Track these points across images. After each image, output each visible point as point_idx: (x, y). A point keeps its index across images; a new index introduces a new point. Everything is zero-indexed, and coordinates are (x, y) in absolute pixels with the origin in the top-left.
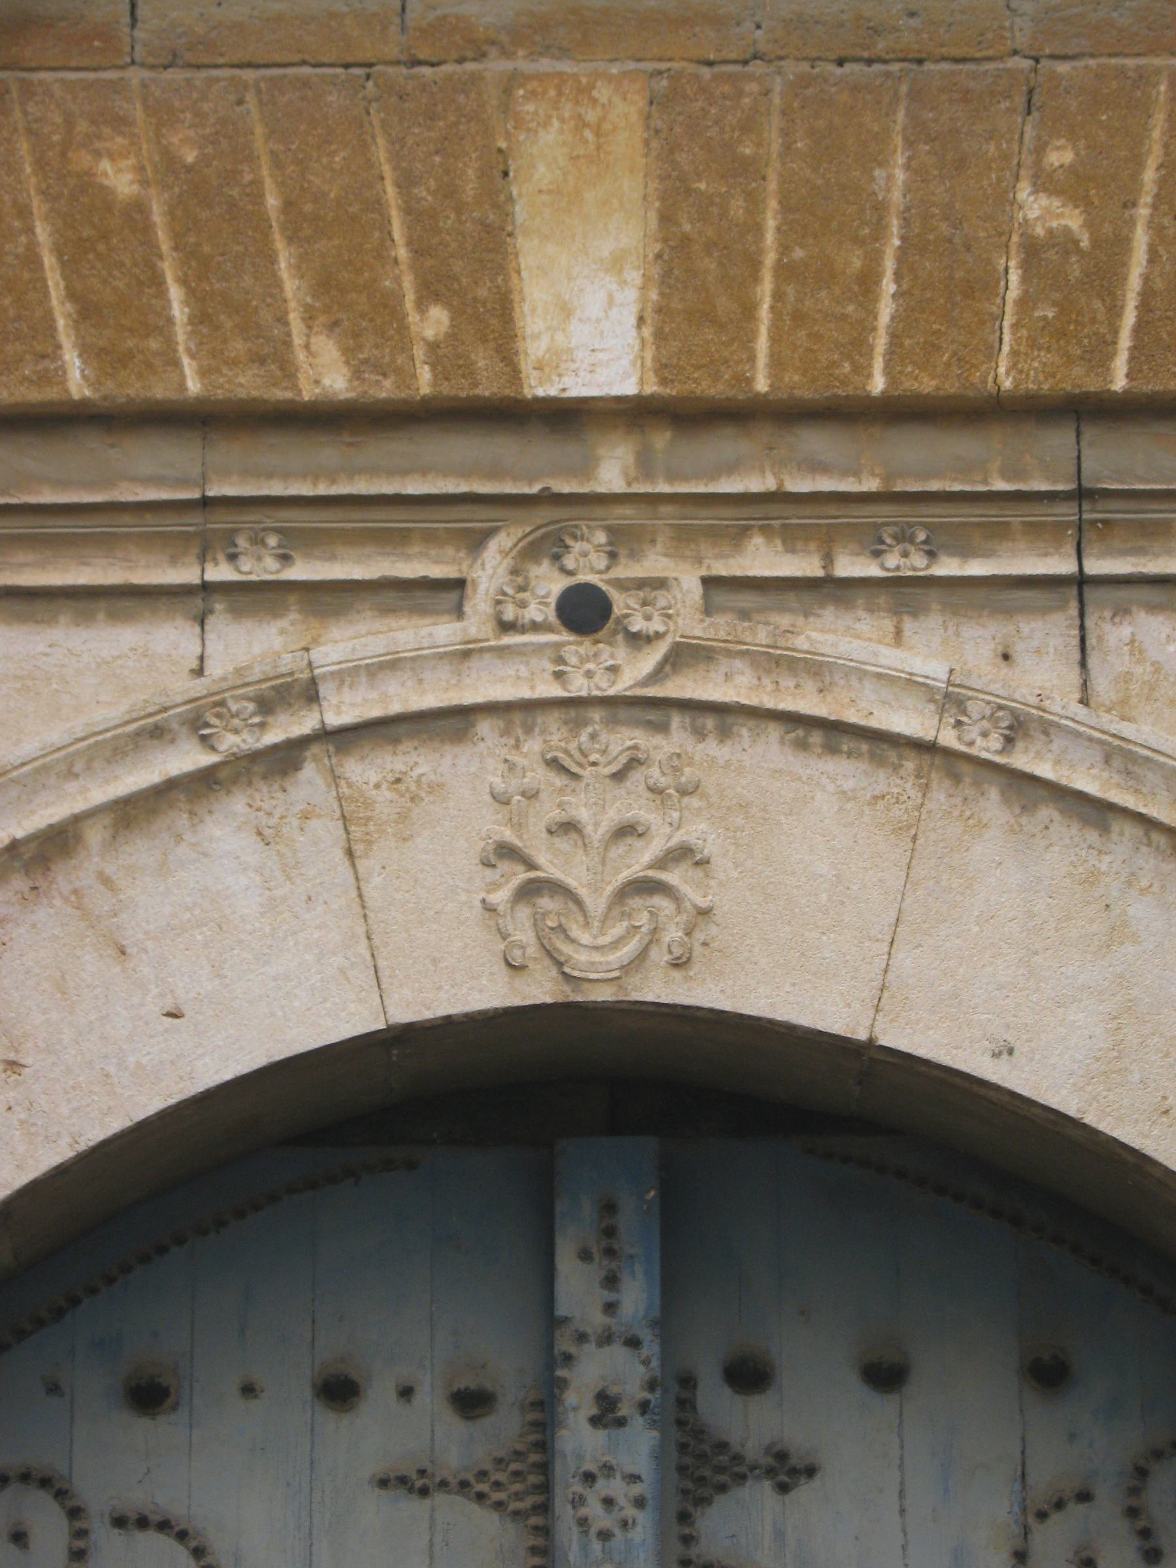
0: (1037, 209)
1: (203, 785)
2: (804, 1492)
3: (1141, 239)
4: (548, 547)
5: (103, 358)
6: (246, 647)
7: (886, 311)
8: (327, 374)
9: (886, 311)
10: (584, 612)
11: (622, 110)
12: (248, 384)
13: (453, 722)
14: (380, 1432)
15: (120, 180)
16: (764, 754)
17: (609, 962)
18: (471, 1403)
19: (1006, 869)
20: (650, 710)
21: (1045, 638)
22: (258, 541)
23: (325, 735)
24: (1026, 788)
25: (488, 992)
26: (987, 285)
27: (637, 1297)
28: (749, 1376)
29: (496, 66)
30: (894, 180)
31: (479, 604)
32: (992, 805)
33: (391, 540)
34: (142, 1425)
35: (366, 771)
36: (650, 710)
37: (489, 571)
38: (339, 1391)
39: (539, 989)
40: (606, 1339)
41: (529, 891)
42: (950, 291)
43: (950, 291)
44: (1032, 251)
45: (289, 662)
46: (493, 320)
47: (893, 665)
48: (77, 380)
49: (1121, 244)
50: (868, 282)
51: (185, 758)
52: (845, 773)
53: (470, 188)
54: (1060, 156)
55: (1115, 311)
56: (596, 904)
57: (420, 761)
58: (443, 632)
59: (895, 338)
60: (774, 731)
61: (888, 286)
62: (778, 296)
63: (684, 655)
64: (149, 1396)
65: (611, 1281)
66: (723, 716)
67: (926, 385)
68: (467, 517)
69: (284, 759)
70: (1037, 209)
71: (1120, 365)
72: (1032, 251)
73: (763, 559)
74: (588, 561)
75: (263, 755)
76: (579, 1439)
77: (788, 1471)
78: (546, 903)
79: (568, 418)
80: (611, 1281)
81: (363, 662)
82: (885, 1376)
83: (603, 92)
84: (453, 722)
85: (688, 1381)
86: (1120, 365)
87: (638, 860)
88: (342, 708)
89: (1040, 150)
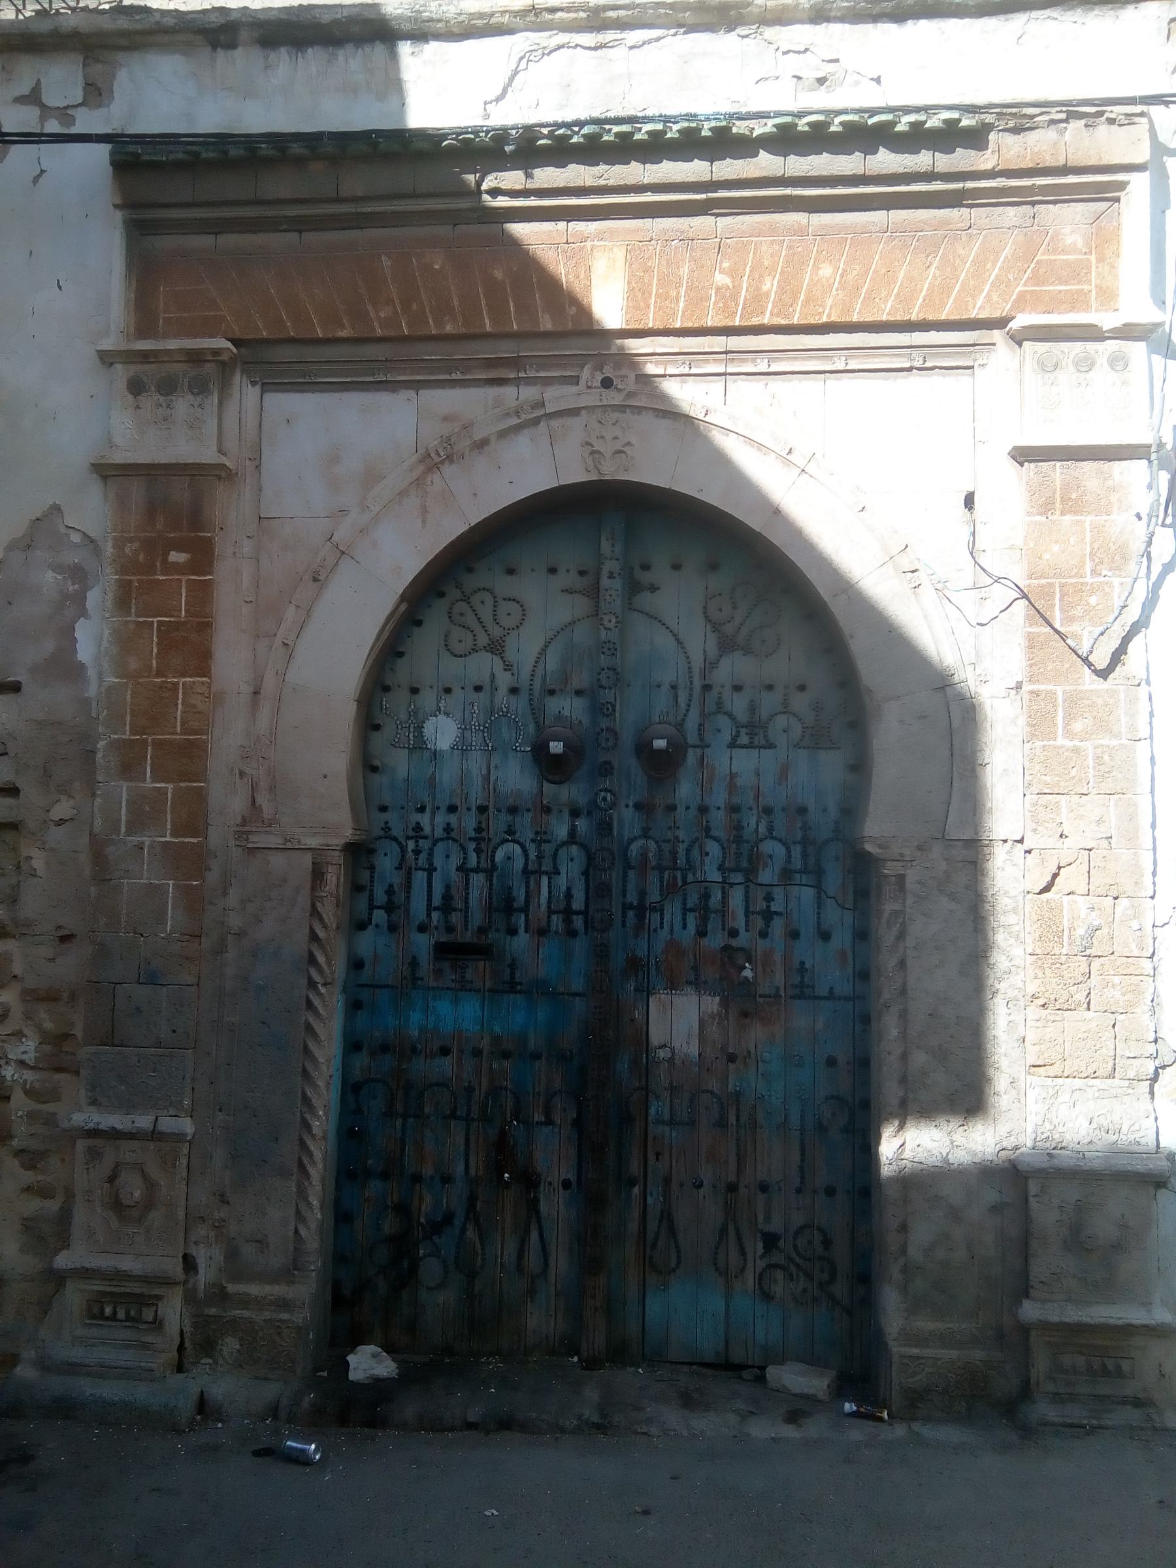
0: (721, 279)
1: (518, 428)
2: (657, 592)
3: (745, 286)
6: (528, 393)
7: (682, 305)
9: (682, 305)
10: (607, 383)
11: (619, 254)
13: (575, 412)
15: (498, 274)
17: (612, 471)
18: (582, 573)
20: (621, 408)
22: (531, 366)
23: (545, 415)
25: (580, 477)
26: (708, 299)
27: (618, 549)
28: (646, 567)
29: (589, 244)
30: (685, 271)
31: (582, 382)
33: (562, 366)
34: (509, 578)
35: (555, 423)
36: (621, 408)
37: (586, 373)
38: (553, 571)
39: (593, 477)
40: (611, 559)
41: (593, 453)
44: (718, 289)
45: (538, 397)
48: (488, 328)
49: (740, 286)
50: (677, 298)
51: (514, 421)
53: (582, 276)
54: (726, 265)
55: (737, 305)
56: (608, 456)
57: (569, 421)
59: (684, 312)
60: (651, 413)
61: (682, 299)
62: (656, 302)
63: (631, 395)
64: (511, 572)
65: (613, 546)
66: (639, 410)
67: (690, 325)
68: (581, 361)
69: (536, 422)
71: (738, 319)
72: (718, 289)
74: (608, 372)
76: (605, 582)
77: (654, 589)
78: (596, 456)
80: (613, 546)
81: (557, 397)
82: (676, 567)
83: (615, 249)
84: (575, 412)
85: (632, 568)
86: (738, 319)
87: (618, 445)
88: (550, 409)
89: (721, 263)
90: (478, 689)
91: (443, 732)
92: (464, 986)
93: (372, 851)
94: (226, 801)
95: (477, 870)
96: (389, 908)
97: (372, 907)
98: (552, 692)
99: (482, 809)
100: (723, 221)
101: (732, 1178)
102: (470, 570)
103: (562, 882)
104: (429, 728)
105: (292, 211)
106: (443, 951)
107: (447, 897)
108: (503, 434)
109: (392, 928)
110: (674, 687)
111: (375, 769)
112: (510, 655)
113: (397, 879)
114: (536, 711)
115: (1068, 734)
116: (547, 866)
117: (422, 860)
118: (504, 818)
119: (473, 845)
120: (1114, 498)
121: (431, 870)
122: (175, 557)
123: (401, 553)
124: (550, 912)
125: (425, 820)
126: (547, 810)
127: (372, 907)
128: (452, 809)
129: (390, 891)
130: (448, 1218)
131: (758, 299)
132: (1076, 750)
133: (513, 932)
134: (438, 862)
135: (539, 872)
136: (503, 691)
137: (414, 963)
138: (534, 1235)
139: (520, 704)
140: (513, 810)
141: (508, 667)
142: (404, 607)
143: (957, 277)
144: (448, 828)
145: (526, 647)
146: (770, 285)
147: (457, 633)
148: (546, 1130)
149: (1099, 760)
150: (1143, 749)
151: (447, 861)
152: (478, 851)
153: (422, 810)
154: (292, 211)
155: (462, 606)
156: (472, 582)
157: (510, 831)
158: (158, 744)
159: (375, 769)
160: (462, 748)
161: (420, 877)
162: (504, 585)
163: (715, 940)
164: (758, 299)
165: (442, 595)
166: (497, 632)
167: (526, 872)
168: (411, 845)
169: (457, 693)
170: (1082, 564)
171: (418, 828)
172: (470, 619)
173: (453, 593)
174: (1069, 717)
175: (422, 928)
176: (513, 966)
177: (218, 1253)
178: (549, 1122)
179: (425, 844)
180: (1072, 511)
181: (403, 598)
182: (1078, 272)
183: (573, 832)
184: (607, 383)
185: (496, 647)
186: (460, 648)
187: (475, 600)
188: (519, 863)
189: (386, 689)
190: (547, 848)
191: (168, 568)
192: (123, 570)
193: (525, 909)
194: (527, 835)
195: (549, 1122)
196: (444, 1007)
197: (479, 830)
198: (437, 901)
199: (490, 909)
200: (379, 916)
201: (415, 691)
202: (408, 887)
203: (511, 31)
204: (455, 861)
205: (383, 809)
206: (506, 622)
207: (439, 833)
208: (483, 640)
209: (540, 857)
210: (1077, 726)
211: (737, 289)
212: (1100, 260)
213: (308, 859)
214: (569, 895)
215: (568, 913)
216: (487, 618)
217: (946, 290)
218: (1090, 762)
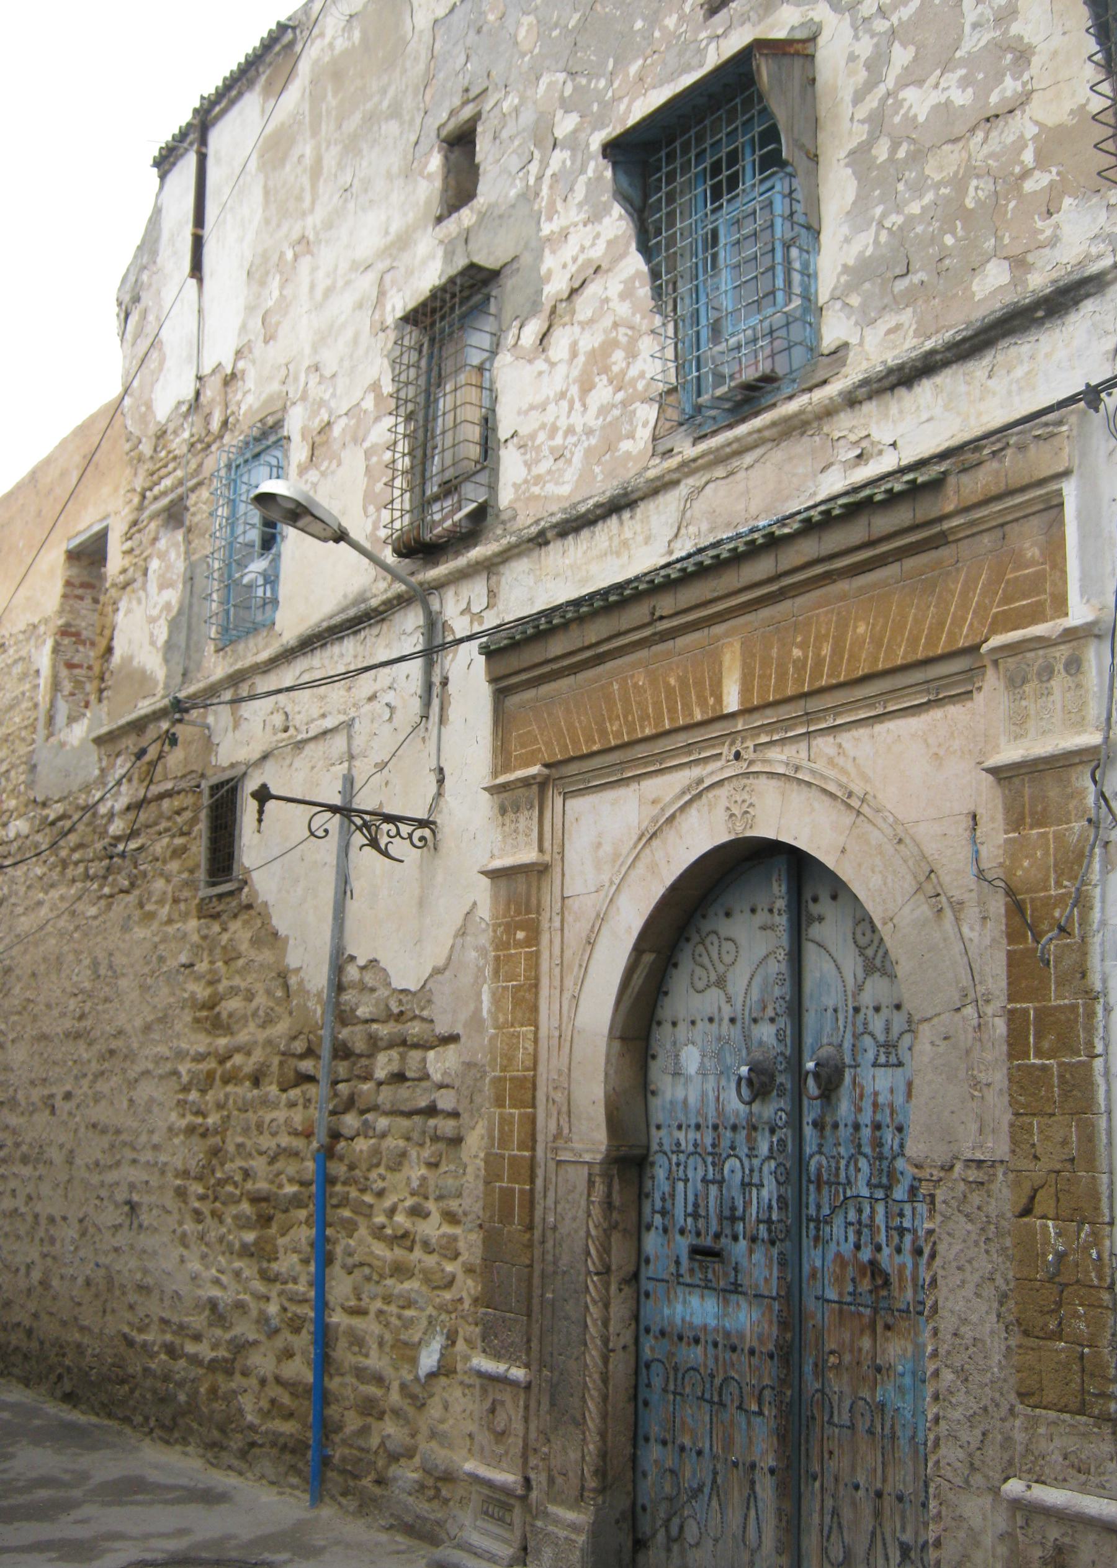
0: (797, 653)
4: (733, 743)
5: (671, 719)
8: (698, 716)
11: (737, 646)
12: (689, 721)
14: (762, 917)
15: (672, 681)
16: (763, 779)
19: (798, 797)
20: (746, 775)
21: (803, 745)
24: (800, 781)
25: (725, 838)
27: (784, 888)
30: (774, 652)
32: (795, 786)
35: (711, 795)
36: (746, 775)
37: (725, 750)
38: (753, 911)
42: (782, 676)
43: (782, 676)
46: (719, 699)
47: (779, 758)
51: (687, 797)
52: (774, 783)
58: (719, 764)
63: (751, 763)
64: (728, 915)
69: (699, 795)
70: (797, 653)
73: (764, 739)
74: (738, 746)
75: (697, 794)
77: (821, 919)
79: (733, 716)
81: (710, 772)
84: (720, 783)
87: (744, 808)
90: (711, 1020)
91: (691, 1059)
92: (707, 1286)
93: (652, 1164)
94: (546, 1125)
95: (713, 1182)
96: (664, 1213)
97: (654, 1212)
98: (755, 1021)
99: (715, 1127)
100: (799, 601)
101: (879, 1485)
102: (704, 917)
103: (765, 1193)
104: (683, 1054)
105: (566, 662)
106: (696, 1251)
107: (696, 1205)
108: (683, 808)
109: (665, 1230)
110: (835, 1011)
111: (653, 1093)
112: (730, 989)
113: (667, 1189)
114: (747, 1037)
115: (1039, 1054)
116: (755, 1180)
117: (681, 1174)
118: (729, 1134)
119: (710, 1159)
120: (1072, 804)
121: (686, 1181)
122: (520, 935)
123: (631, 916)
124: (759, 1221)
125: (681, 1136)
126: (755, 1128)
127: (654, 1212)
128: (698, 1127)
129: (663, 1199)
130: (700, 1489)
131: (819, 662)
132: (1044, 1068)
133: (735, 1238)
134: (690, 1175)
135: (750, 1184)
136: (726, 1021)
137: (678, 1263)
138: (752, 1513)
139: (736, 1032)
140: (734, 1128)
141: (729, 1000)
142: (648, 958)
143: (948, 610)
144: (696, 1145)
145: (738, 981)
146: (826, 650)
147: (699, 971)
148: (759, 1419)
149: (1061, 1076)
150: (1098, 1063)
151: (696, 1174)
152: (714, 1164)
153: (680, 1127)
154: (566, 662)
155: (700, 948)
156: (706, 926)
157: (733, 1148)
158: (512, 1079)
159: (653, 1093)
160: (703, 1073)
161: (680, 1185)
162: (726, 928)
163: (865, 1255)
164: (819, 662)
165: (688, 940)
166: (721, 968)
167: (744, 1185)
168: (674, 1158)
169: (699, 1024)
170: (1046, 879)
171: (678, 1144)
172: (705, 960)
173: (696, 938)
174: (1039, 1036)
175: (682, 1232)
176: (736, 1270)
177: (544, 1477)
178: (760, 1413)
179: (682, 1157)
180: (1039, 824)
181: (639, 949)
182: (1036, 584)
183: (771, 1149)
184: (738, 756)
185: (721, 983)
186: (700, 985)
187: (708, 942)
188: (739, 1175)
189: (659, 1023)
190: (756, 1162)
191: (518, 944)
192: (497, 949)
193: (743, 1219)
194: (743, 1150)
195: (760, 1413)
196: (695, 1301)
197: (714, 1145)
198: (690, 1209)
199: (721, 1218)
200: (658, 1219)
201: (674, 1024)
202: (673, 1196)
203: (675, 483)
204: (700, 1173)
205: (658, 1127)
206: (728, 959)
207: (691, 1148)
208: (713, 977)
209: (752, 1171)
210: (1046, 1045)
211: (806, 657)
212: (1053, 568)
213: (585, 1171)
214: (770, 1207)
215: (769, 1221)
216: (715, 956)
217: (941, 624)
218: (1056, 1080)
